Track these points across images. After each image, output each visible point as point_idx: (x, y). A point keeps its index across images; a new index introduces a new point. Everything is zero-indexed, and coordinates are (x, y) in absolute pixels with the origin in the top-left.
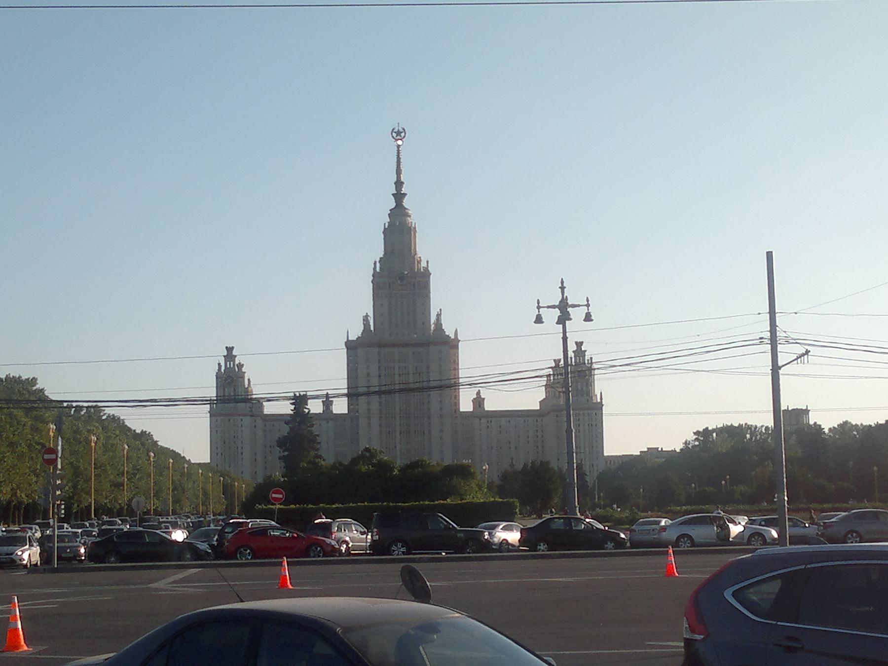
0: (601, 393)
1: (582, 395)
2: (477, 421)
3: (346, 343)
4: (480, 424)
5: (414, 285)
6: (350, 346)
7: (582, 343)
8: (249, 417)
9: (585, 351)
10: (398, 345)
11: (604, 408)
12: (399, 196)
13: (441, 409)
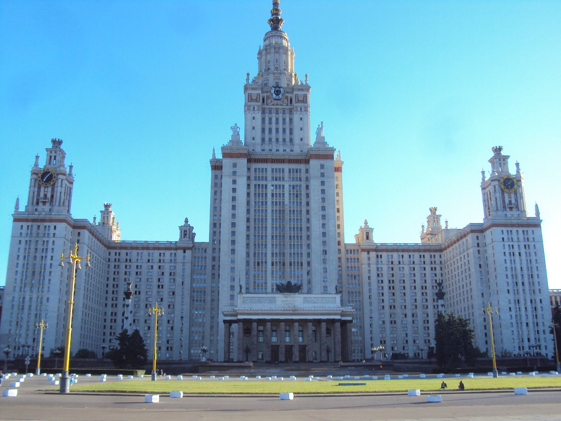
0: (536, 206)
1: (511, 209)
2: (365, 254)
3: (211, 162)
4: (369, 258)
5: (291, 100)
6: (216, 166)
7: (500, 149)
8: (64, 225)
9: (508, 157)
10: (274, 161)
11: (542, 224)
12: (275, 22)
13: (324, 234)
